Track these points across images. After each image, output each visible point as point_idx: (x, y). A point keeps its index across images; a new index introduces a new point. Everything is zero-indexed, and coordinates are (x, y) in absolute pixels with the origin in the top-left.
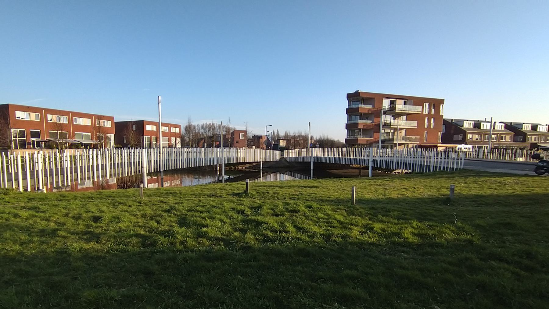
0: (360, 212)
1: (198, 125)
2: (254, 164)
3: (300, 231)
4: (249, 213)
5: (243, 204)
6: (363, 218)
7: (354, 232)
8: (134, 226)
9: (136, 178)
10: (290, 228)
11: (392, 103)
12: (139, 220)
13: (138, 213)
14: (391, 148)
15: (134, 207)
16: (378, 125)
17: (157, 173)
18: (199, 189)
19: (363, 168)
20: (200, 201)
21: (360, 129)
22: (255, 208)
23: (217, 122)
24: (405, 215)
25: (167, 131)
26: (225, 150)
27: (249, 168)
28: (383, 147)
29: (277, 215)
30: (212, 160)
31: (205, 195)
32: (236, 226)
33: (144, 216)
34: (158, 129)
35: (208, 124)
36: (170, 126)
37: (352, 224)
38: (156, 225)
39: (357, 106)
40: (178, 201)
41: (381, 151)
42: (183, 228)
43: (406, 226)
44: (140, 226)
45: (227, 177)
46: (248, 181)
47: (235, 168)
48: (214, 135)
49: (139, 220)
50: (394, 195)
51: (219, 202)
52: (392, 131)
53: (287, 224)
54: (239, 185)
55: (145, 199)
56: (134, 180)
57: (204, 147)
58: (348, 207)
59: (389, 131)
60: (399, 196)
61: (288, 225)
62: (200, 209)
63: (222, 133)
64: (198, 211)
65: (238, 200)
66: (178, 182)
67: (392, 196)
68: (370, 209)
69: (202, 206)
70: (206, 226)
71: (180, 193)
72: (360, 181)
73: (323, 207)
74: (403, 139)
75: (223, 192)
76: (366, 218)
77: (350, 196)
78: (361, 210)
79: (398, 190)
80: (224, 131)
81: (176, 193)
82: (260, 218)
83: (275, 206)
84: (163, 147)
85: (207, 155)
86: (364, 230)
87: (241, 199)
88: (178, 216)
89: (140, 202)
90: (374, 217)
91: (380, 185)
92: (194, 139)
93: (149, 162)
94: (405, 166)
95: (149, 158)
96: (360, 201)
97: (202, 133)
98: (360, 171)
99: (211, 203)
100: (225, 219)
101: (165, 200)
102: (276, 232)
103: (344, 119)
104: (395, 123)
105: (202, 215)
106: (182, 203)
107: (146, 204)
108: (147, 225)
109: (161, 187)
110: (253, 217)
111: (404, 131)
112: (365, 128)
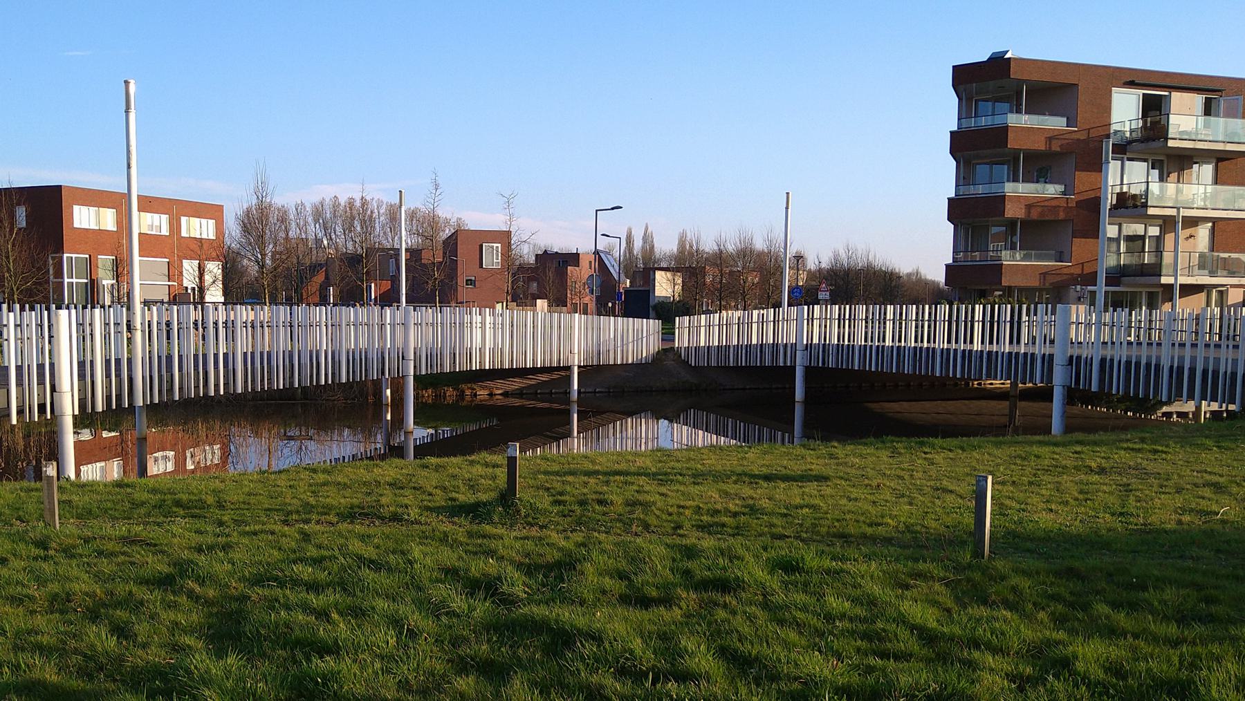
0: (1014, 589)
1: (300, 208)
2: (544, 378)
3: (744, 674)
4: (519, 591)
5: (491, 553)
6: (1025, 616)
7: (987, 678)
8: (17, 648)
9: (27, 436)
10: (702, 658)
11: (1154, 108)
12: (40, 621)
13: (33, 591)
14: (1152, 306)
15: (16, 564)
16: (1092, 205)
17: (118, 414)
18: (302, 486)
19: (1028, 395)
20: (306, 537)
21: (1012, 223)
22: (549, 567)
23: (380, 194)
24: (1209, 600)
25: (165, 231)
26: (414, 315)
27: (520, 394)
28: (1116, 302)
29: (645, 602)
30: (358, 359)
31: (327, 510)
32: (464, 650)
33: (60, 603)
34: (124, 221)
35: (343, 201)
36: (176, 209)
37: (975, 644)
38: (112, 642)
39: (998, 120)
40: (210, 540)
41: (1107, 317)
42: (231, 660)
43: (1216, 649)
44: (40, 649)
45: (421, 434)
46: (515, 449)
47: (462, 395)
48: (371, 251)
49: (40, 621)
50: (1164, 512)
51: (391, 545)
52: (1154, 231)
53: (687, 643)
54: (479, 470)
55: (63, 528)
56: (21, 447)
57: (323, 301)
58: (959, 568)
59: (1138, 229)
60: (1186, 518)
61: (691, 646)
62: (305, 572)
63: (405, 240)
64: (296, 582)
65: (470, 535)
66: (211, 454)
67: (1153, 519)
68: (1058, 574)
69: (317, 562)
70: (331, 649)
71: (221, 505)
72: (1012, 450)
73: (848, 566)
74: (1202, 266)
75: (409, 498)
76: (1041, 615)
77: (969, 520)
78: (1015, 580)
79: (1179, 491)
80: (410, 232)
81: (203, 505)
82: (566, 615)
83: (633, 560)
84: (146, 303)
85: (335, 335)
86: (1029, 670)
87: (488, 528)
88: (209, 603)
89: (42, 544)
90: (1074, 613)
91: (1102, 471)
92: (280, 267)
93: (84, 370)
94: (1211, 383)
95: (82, 350)
96: (1014, 541)
97: (318, 241)
98: (1013, 408)
99: (356, 546)
100: (415, 618)
101: (153, 533)
102: (639, 676)
103: (941, 177)
104: (1165, 195)
105: (314, 600)
106: (226, 548)
107: (68, 552)
108: (73, 643)
109: (133, 478)
110: (539, 611)
111: (1203, 232)
112: (1035, 215)
